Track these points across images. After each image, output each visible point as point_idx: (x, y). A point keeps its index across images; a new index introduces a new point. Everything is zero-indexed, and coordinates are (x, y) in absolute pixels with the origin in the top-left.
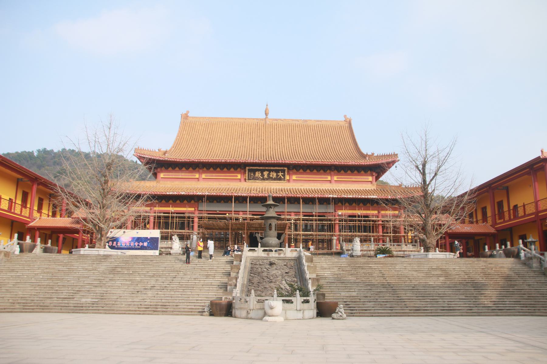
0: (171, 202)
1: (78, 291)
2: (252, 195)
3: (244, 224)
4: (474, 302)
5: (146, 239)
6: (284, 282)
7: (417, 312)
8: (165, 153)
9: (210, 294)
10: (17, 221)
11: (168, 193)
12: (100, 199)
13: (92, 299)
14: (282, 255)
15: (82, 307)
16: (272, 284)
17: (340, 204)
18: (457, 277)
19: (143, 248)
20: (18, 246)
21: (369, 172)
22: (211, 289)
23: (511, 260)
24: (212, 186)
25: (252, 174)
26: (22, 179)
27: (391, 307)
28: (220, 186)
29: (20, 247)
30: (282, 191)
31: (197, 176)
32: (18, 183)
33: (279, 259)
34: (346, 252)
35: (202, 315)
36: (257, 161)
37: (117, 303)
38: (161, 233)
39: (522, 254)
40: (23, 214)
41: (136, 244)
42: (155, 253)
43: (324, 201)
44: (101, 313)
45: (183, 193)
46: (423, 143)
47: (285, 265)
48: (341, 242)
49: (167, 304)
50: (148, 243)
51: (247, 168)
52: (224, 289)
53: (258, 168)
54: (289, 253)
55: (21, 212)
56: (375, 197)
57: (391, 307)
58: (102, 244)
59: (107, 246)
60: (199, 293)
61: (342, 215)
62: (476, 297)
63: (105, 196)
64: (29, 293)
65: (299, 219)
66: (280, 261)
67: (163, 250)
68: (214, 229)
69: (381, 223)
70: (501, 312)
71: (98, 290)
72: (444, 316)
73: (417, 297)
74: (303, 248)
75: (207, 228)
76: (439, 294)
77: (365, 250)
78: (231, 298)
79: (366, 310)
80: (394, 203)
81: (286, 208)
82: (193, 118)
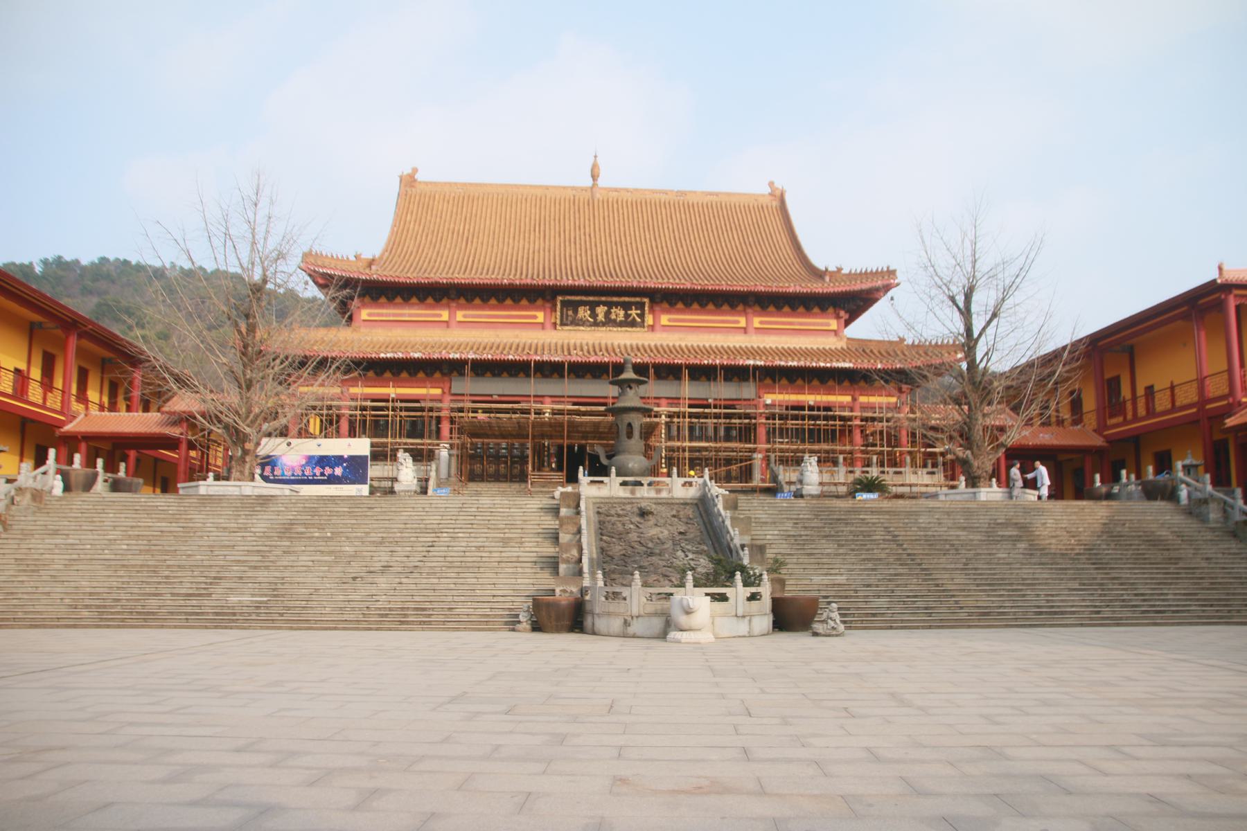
0: (388, 375)
1: (215, 578)
2: (574, 359)
3: (561, 425)
4: (1101, 595)
5: (339, 460)
6: (680, 553)
7: (985, 618)
8: (371, 263)
9: (519, 581)
10: (33, 421)
11: (382, 355)
12: (238, 368)
13: (253, 595)
14: (664, 495)
15: (234, 614)
16: (654, 559)
17: (768, 381)
18: (1053, 541)
19: (332, 480)
20: (59, 477)
21: (831, 310)
22: (520, 570)
23: (1159, 504)
24: (479, 340)
25: (570, 313)
26: (41, 323)
27: (926, 608)
28: (498, 340)
29: (63, 480)
30: (638, 349)
31: (445, 315)
32: (32, 333)
33: (659, 502)
34: (786, 488)
35: (513, 630)
36: (582, 282)
37: (311, 604)
38: (372, 445)
39: (1183, 493)
40: (48, 404)
41: (318, 471)
42: (359, 490)
43: (736, 374)
44: (280, 628)
45: (417, 355)
46: (967, 244)
47: (674, 516)
48: (772, 465)
49: (428, 605)
50: (345, 469)
51: (560, 298)
52: (549, 570)
53: (584, 298)
54: (680, 488)
55: (45, 399)
56: (847, 365)
57: (926, 608)
58: (247, 472)
59: (257, 477)
60: (494, 581)
61: (773, 405)
62: (1102, 584)
63: (251, 361)
64: (106, 584)
65: (678, 415)
66: (660, 508)
67: (376, 484)
68: (488, 436)
69: (858, 422)
70: (1162, 618)
71: (262, 575)
72: (1043, 626)
73: (978, 585)
74: (711, 479)
75: (473, 435)
76: (1024, 579)
77: (829, 484)
78: (575, 590)
79: (874, 615)
80: (900, 379)
81: (654, 388)
82: (426, 183)
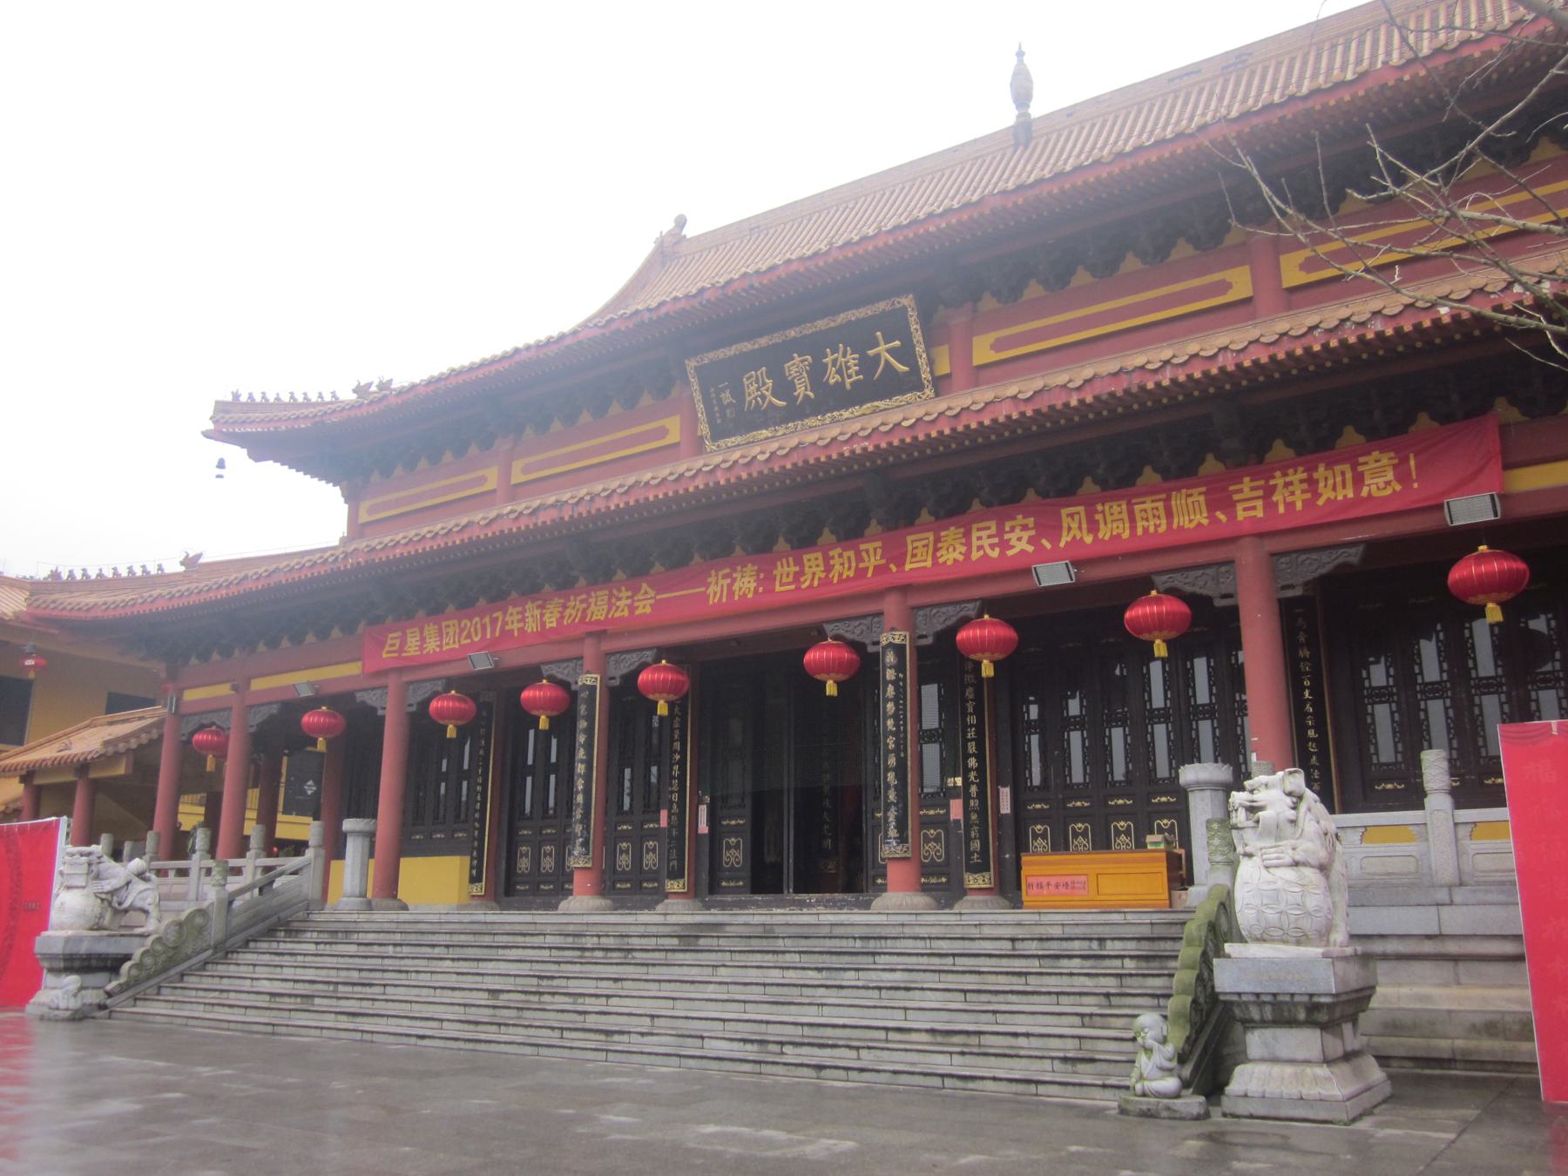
51: (691, 364)
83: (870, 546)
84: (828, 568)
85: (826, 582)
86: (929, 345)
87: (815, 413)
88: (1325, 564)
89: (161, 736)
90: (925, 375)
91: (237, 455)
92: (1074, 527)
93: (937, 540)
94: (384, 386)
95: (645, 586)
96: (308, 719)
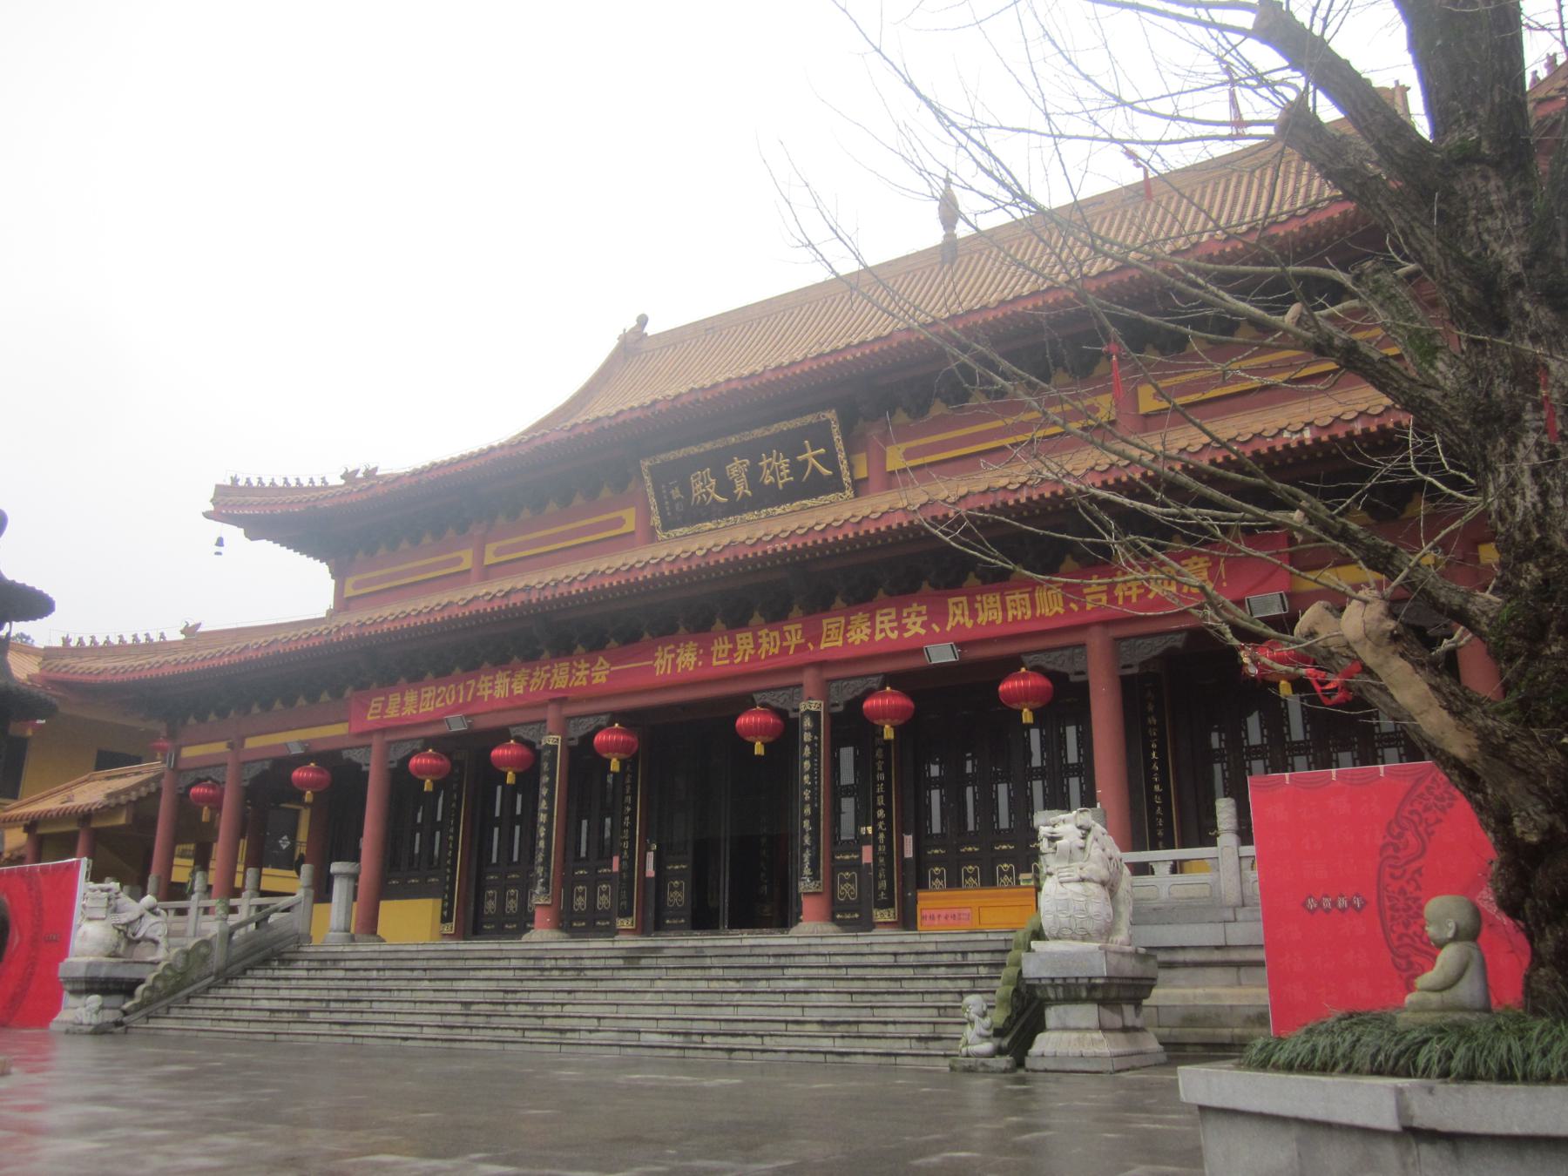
51: (646, 464)
83: (792, 628)
84: (757, 646)
85: (755, 658)
86: (850, 452)
87: (752, 509)
88: (1157, 647)
89: (159, 790)
90: (846, 479)
91: (234, 534)
92: (958, 615)
93: (848, 623)
94: (370, 473)
95: (601, 659)
96: (297, 774)
